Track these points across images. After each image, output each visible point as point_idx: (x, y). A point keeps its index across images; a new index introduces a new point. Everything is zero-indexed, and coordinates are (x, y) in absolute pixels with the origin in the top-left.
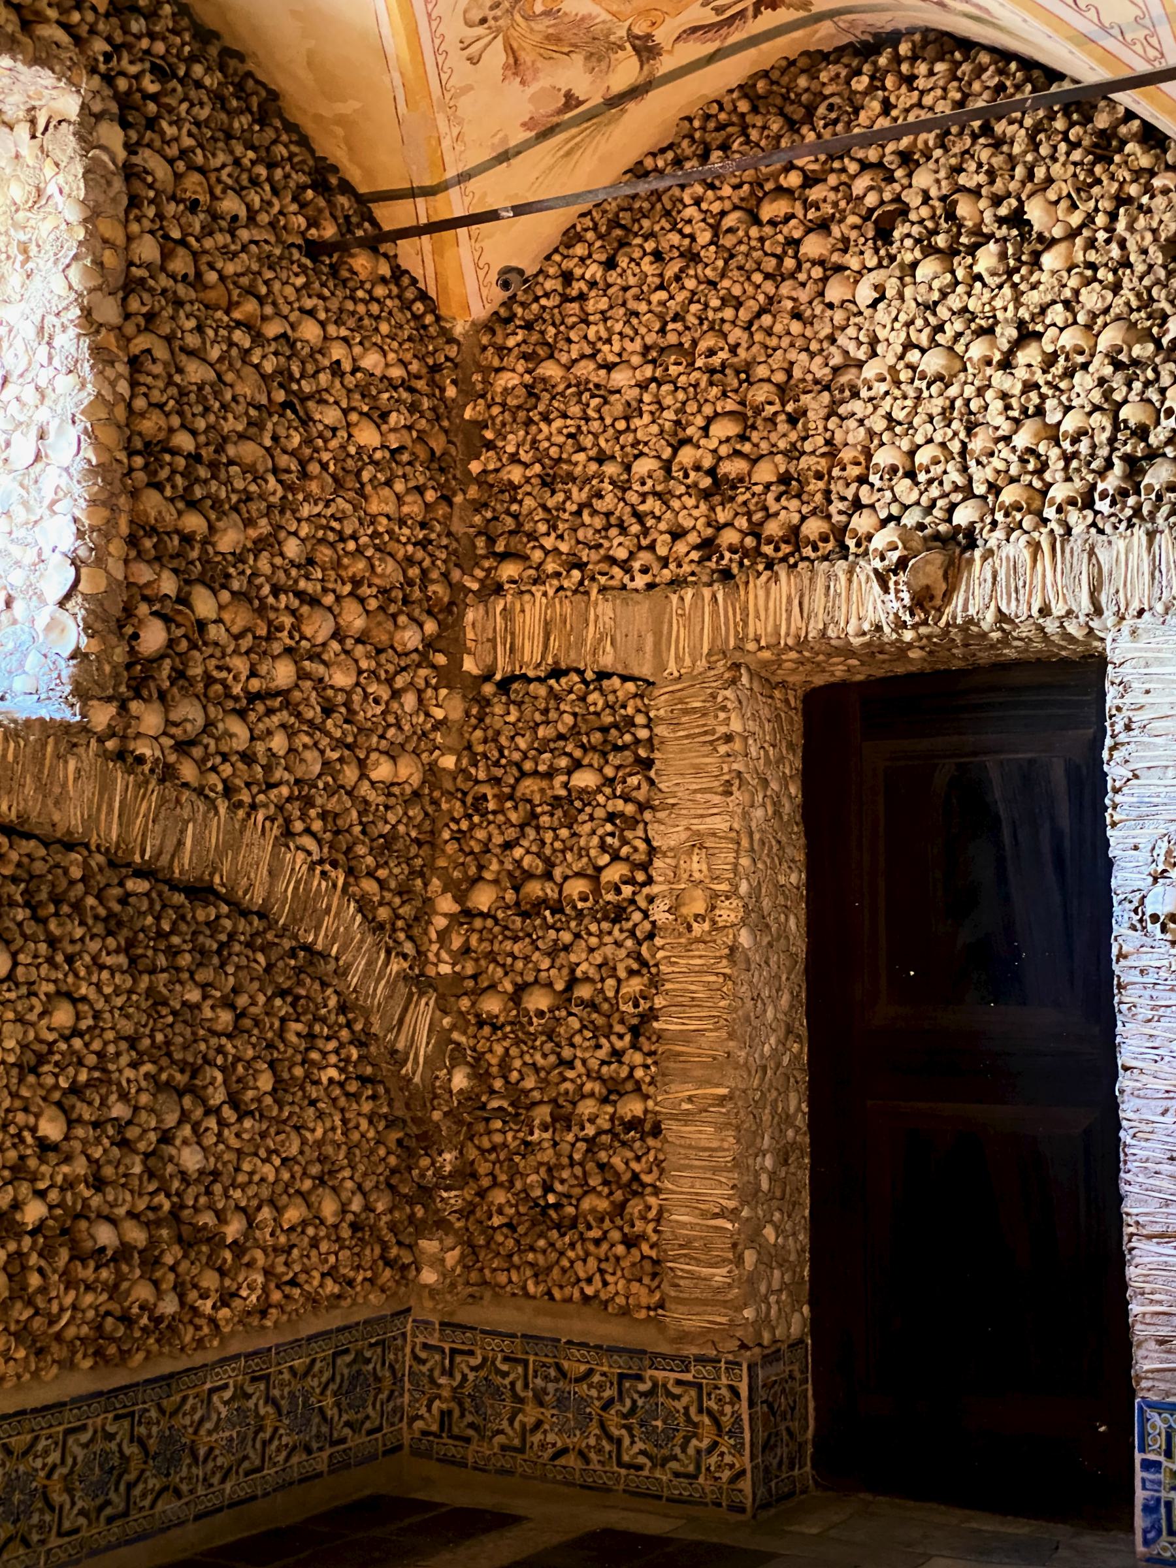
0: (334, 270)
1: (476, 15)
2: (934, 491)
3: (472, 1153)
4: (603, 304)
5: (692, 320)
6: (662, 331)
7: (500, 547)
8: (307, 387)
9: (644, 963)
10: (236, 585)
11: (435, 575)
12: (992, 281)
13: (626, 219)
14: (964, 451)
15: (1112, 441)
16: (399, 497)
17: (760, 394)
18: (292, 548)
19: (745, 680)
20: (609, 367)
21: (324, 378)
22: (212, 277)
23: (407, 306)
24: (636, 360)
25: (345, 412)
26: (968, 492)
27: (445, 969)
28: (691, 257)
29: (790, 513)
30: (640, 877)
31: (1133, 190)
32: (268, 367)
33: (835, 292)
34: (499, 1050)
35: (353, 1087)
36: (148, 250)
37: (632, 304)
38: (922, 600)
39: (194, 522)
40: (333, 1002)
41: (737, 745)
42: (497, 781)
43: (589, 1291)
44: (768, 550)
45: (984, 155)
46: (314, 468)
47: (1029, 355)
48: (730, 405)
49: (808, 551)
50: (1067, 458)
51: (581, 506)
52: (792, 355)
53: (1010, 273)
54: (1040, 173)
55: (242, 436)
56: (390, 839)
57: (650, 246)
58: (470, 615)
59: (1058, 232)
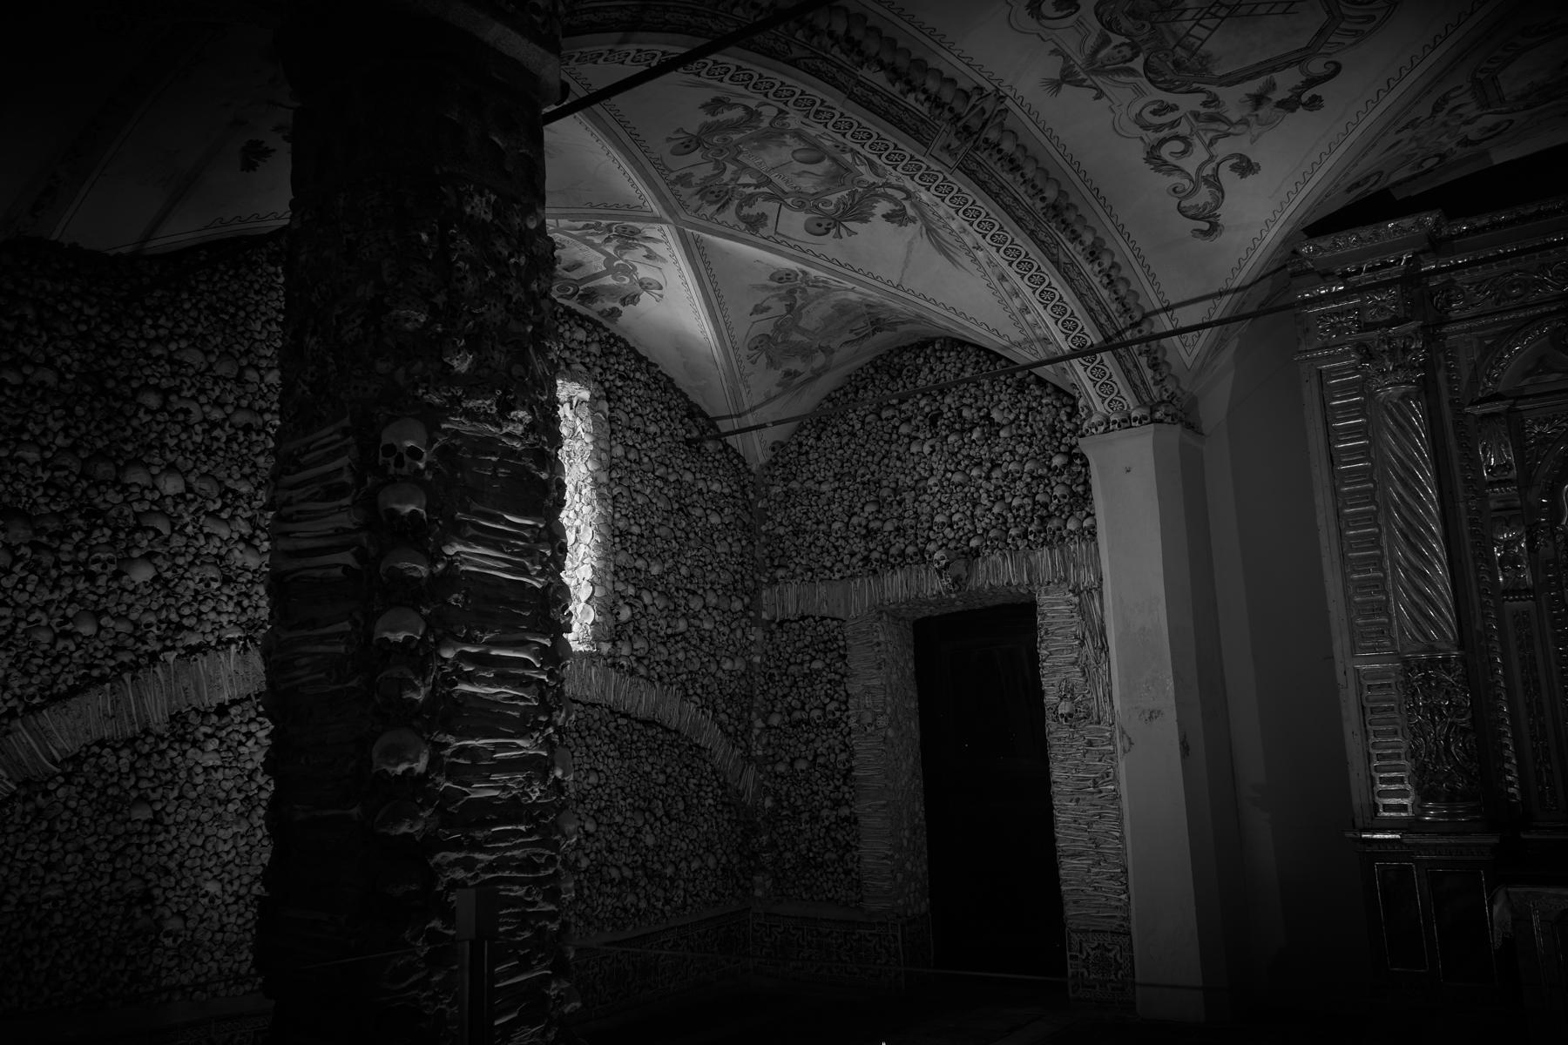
0: (698, 449)
1: (753, 346)
2: (961, 533)
3: (775, 836)
4: (816, 456)
5: (854, 462)
6: (842, 467)
7: (776, 563)
8: (688, 501)
9: (847, 746)
10: (660, 589)
11: (747, 577)
12: (979, 443)
13: (824, 419)
14: (972, 515)
15: (1033, 510)
16: (730, 544)
17: (885, 493)
18: (684, 571)
19: (885, 618)
20: (820, 483)
21: (695, 496)
22: (646, 460)
23: (730, 461)
24: (831, 479)
25: (705, 510)
26: (976, 534)
27: (760, 753)
28: (854, 435)
29: (900, 544)
30: (843, 708)
31: (1034, 404)
32: (671, 494)
33: (914, 449)
34: (785, 788)
35: (719, 807)
36: (619, 451)
37: (829, 456)
38: (957, 580)
39: (640, 563)
40: (709, 769)
41: (883, 647)
42: (778, 667)
43: (830, 896)
44: (892, 560)
45: (973, 390)
46: (692, 535)
47: (996, 474)
48: (872, 498)
49: (909, 560)
50: (1015, 518)
51: (811, 544)
52: (898, 476)
53: (987, 439)
54: (996, 398)
55: (660, 525)
56: (732, 696)
57: (835, 431)
58: (764, 594)
59: (1005, 422)
